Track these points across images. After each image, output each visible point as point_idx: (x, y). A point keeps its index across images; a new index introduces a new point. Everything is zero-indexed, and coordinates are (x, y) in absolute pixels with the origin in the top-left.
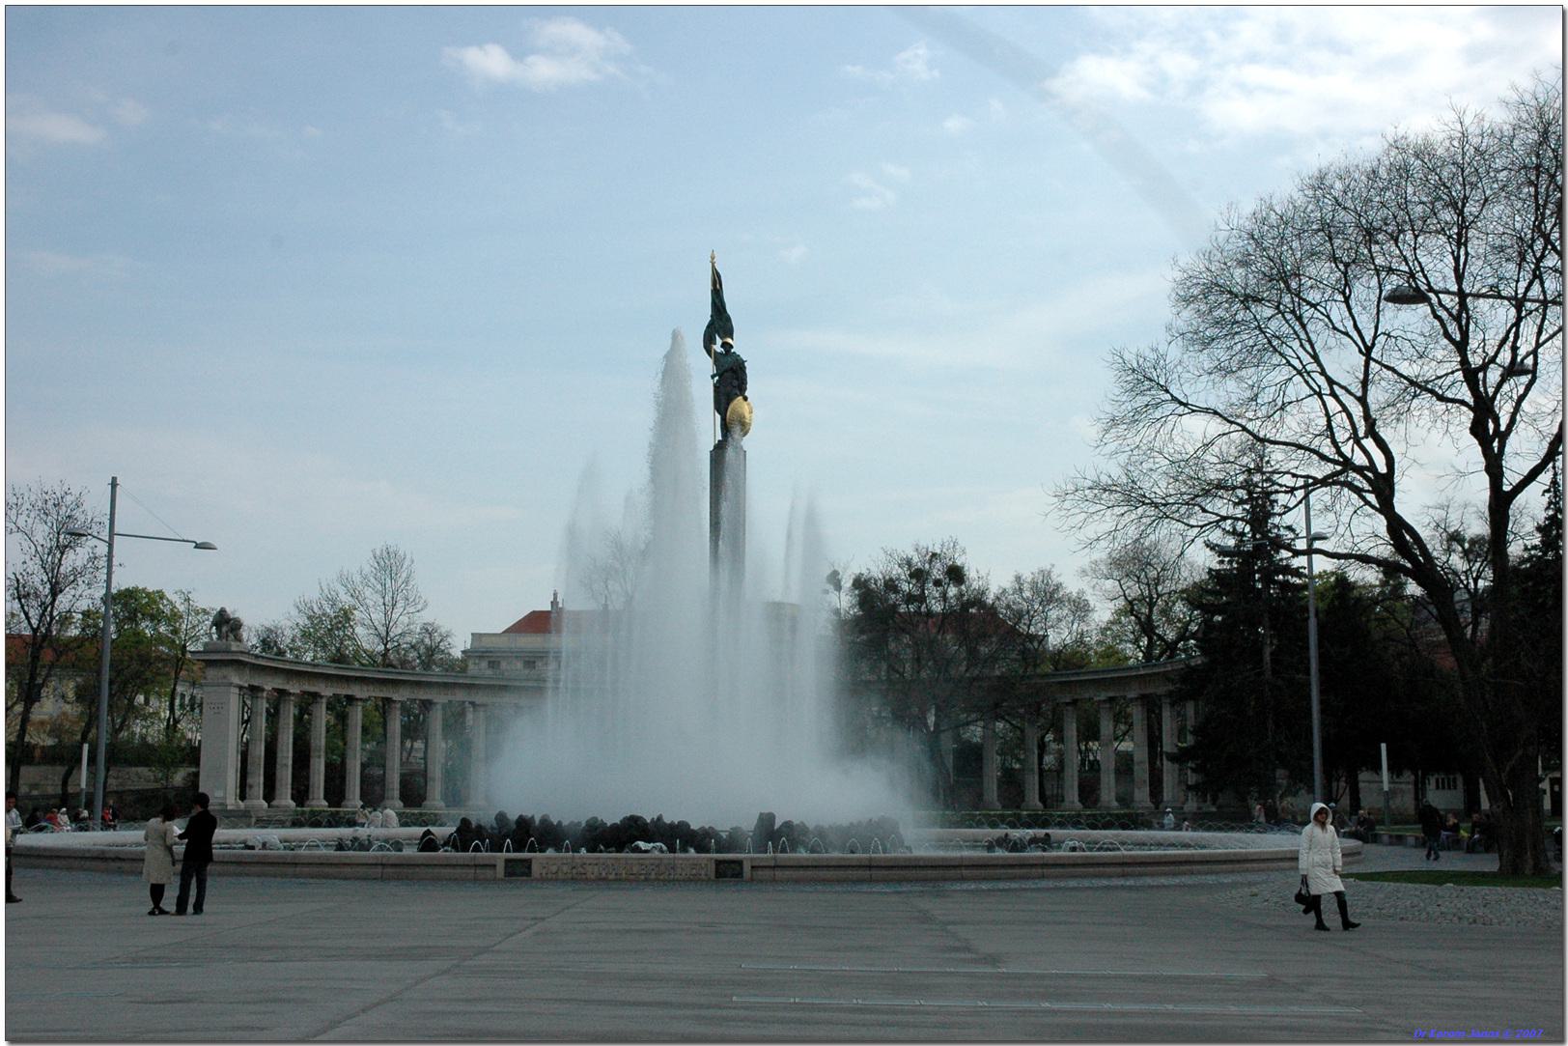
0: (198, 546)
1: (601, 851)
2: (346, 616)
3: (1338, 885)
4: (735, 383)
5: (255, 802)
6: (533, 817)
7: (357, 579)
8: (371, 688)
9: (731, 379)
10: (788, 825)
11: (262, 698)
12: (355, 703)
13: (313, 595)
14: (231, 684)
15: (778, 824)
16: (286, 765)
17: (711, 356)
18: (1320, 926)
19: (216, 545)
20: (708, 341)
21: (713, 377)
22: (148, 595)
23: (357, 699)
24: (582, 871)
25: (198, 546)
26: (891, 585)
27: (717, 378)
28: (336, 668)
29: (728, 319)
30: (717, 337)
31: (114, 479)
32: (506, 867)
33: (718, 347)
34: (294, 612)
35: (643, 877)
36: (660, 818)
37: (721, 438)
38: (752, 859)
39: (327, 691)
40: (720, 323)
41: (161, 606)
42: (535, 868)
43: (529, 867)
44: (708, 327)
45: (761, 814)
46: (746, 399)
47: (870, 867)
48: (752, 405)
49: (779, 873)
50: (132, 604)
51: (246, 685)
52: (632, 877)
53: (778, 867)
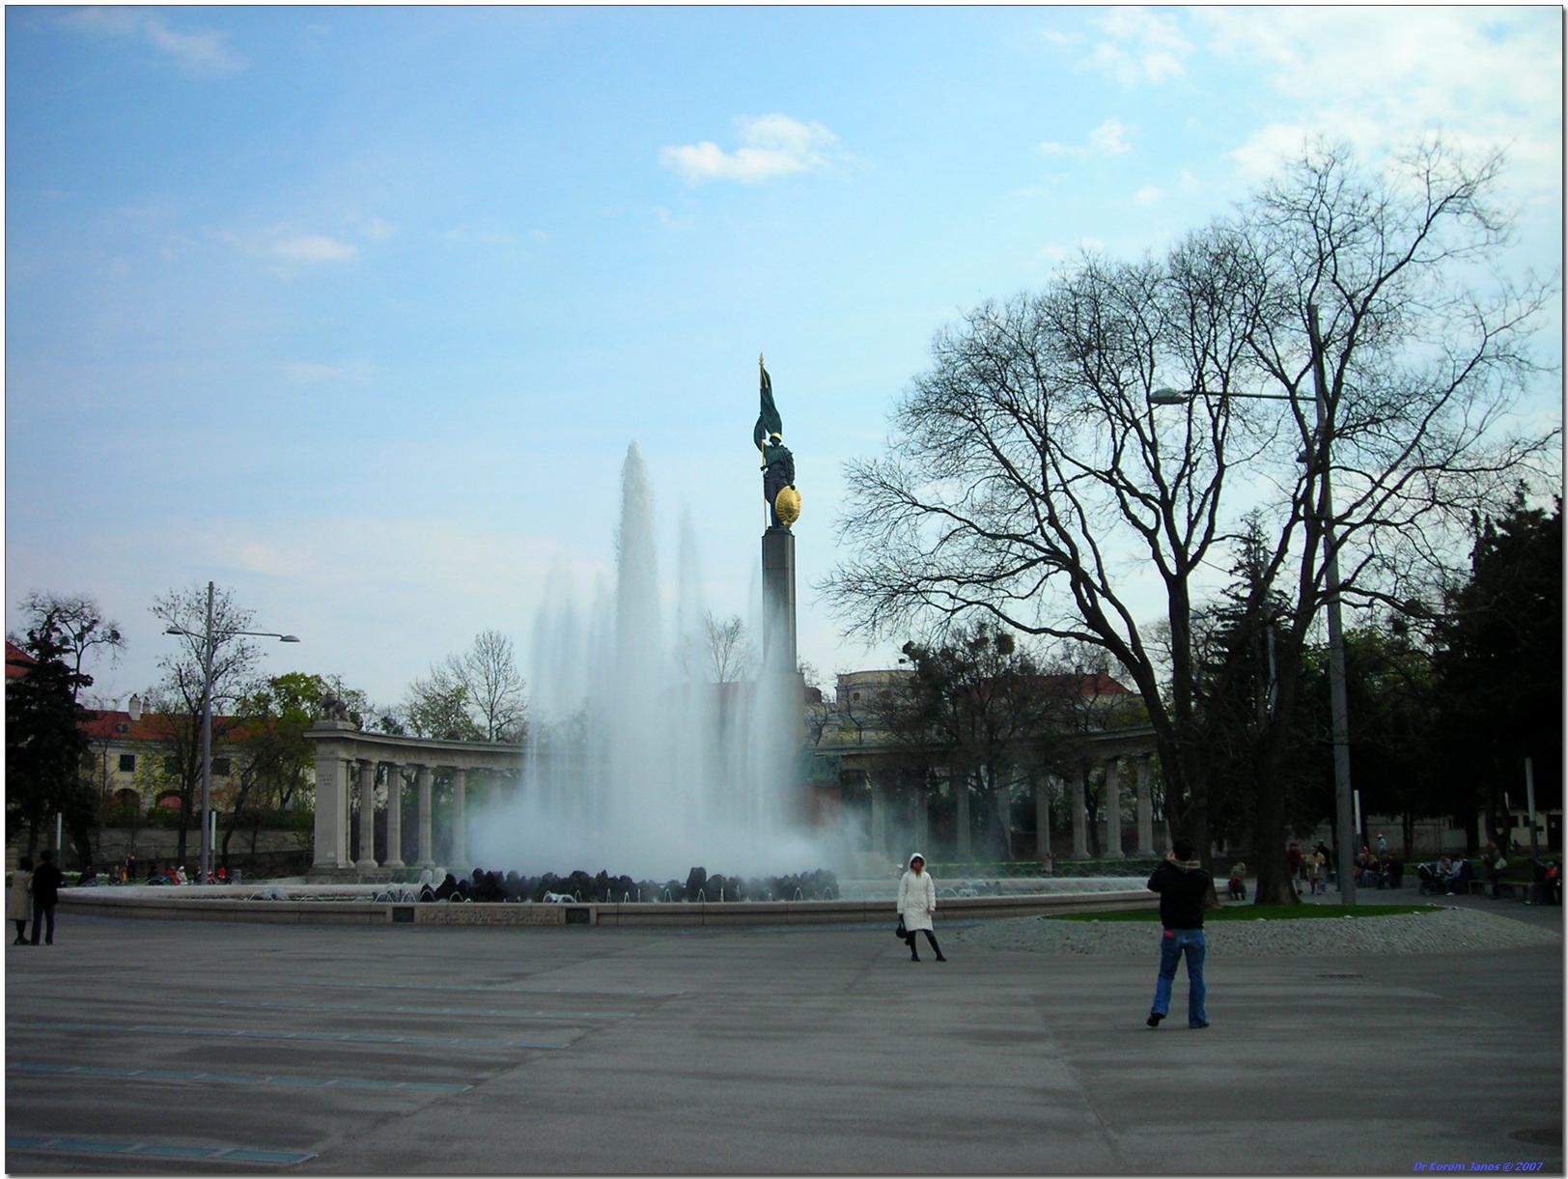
0: (284, 639)
1: (517, 901)
2: (460, 693)
3: (928, 925)
5: (367, 862)
7: (463, 662)
8: (473, 760)
10: (717, 878)
11: (371, 770)
13: (426, 677)
14: (337, 759)
15: (799, 876)
16: (395, 830)
17: (760, 449)
18: (915, 958)
19: (299, 638)
20: (758, 437)
21: (762, 469)
22: (307, 680)
23: (461, 770)
24: (454, 917)
25: (284, 639)
26: (947, 653)
27: (766, 469)
29: (777, 415)
31: (211, 583)
32: (394, 914)
33: (767, 442)
34: (411, 693)
35: (504, 923)
36: (604, 873)
37: (771, 525)
38: (597, 907)
39: (432, 763)
40: (769, 419)
41: (319, 690)
42: (417, 914)
43: (413, 915)
44: (758, 423)
45: (693, 869)
46: (793, 488)
47: (703, 913)
48: (800, 493)
49: (621, 919)
50: (291, 687)
52: (496, 923)
53: (621, 914)
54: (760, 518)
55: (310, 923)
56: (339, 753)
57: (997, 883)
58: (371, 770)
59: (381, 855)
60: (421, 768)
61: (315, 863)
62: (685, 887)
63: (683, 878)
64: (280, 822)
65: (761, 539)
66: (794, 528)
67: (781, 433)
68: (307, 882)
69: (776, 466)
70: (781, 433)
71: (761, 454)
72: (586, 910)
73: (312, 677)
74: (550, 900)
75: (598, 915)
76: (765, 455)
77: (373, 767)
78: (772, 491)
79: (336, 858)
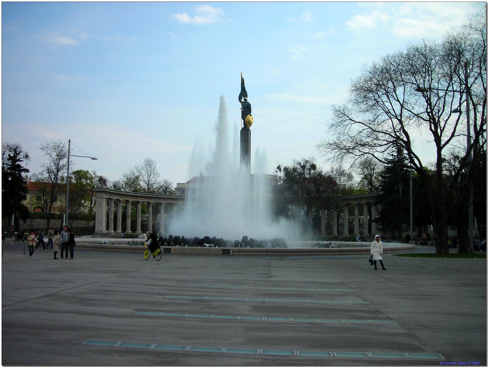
1: (195, 246)
2: (137, 178)
3: (381, 259)
4: (248, 111)
5: (111, 231)
6: (179, 236)
7: (140, 168)
8: (144, 199)
9: (246, 110)
10: (251, 240)
11: (113, 202)
12: (139, 203)
13: (128, 172)
14: (103, 198)
16: (120, 221)
18: (376, 269)
19: (97, 159)
21: (241, 109)
22: (84, 172)
24: (185, 252)
25: (92, 159)
26: (294, 169)
27: (242, 109)
28: (134, 193)
30: (243, 97)
31: (70, 140)
32: (164, 250)
33: (243, 100)
34: (123, 177)
35: (202, 254)
36: (215, 237)
38: (233, 249)
39: (131, 200)
40: (243, 93)
41: (88, 175)
42: (172, 251)
43: (171, 250)
44: (240, 94)
45: (244, 236)
46: (251, 115)
47: (267, 252)
48: (253, 117)
49: (240, 253)
50: (80, 174)
51: (108, 198)
52: (199, 254)
53: (241, 251)
54: (240, 125)
55: (135, 253)
56: (104, 196)
57: (319, 243)
58: (113, 202)
59: (134, 229)
60: (127, 202)
61: (95, 231)
62: (241, 242)
63: (240, 239)
64: (84, 217)
65: (240, 131)
66: (251, 128)
67: (247, 98)
68: (93, 237)
69: (246, 108)
70: (247, 98)
71: (241, 104)
72: (170, 249)
73: (86, 171)
74: (205, 246)
75: (233, 251)
76: (242, 105)
77: (113, 201)
78: (244, 116)
79: (102, 230)
